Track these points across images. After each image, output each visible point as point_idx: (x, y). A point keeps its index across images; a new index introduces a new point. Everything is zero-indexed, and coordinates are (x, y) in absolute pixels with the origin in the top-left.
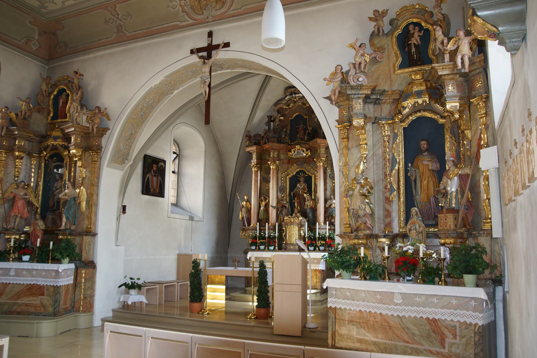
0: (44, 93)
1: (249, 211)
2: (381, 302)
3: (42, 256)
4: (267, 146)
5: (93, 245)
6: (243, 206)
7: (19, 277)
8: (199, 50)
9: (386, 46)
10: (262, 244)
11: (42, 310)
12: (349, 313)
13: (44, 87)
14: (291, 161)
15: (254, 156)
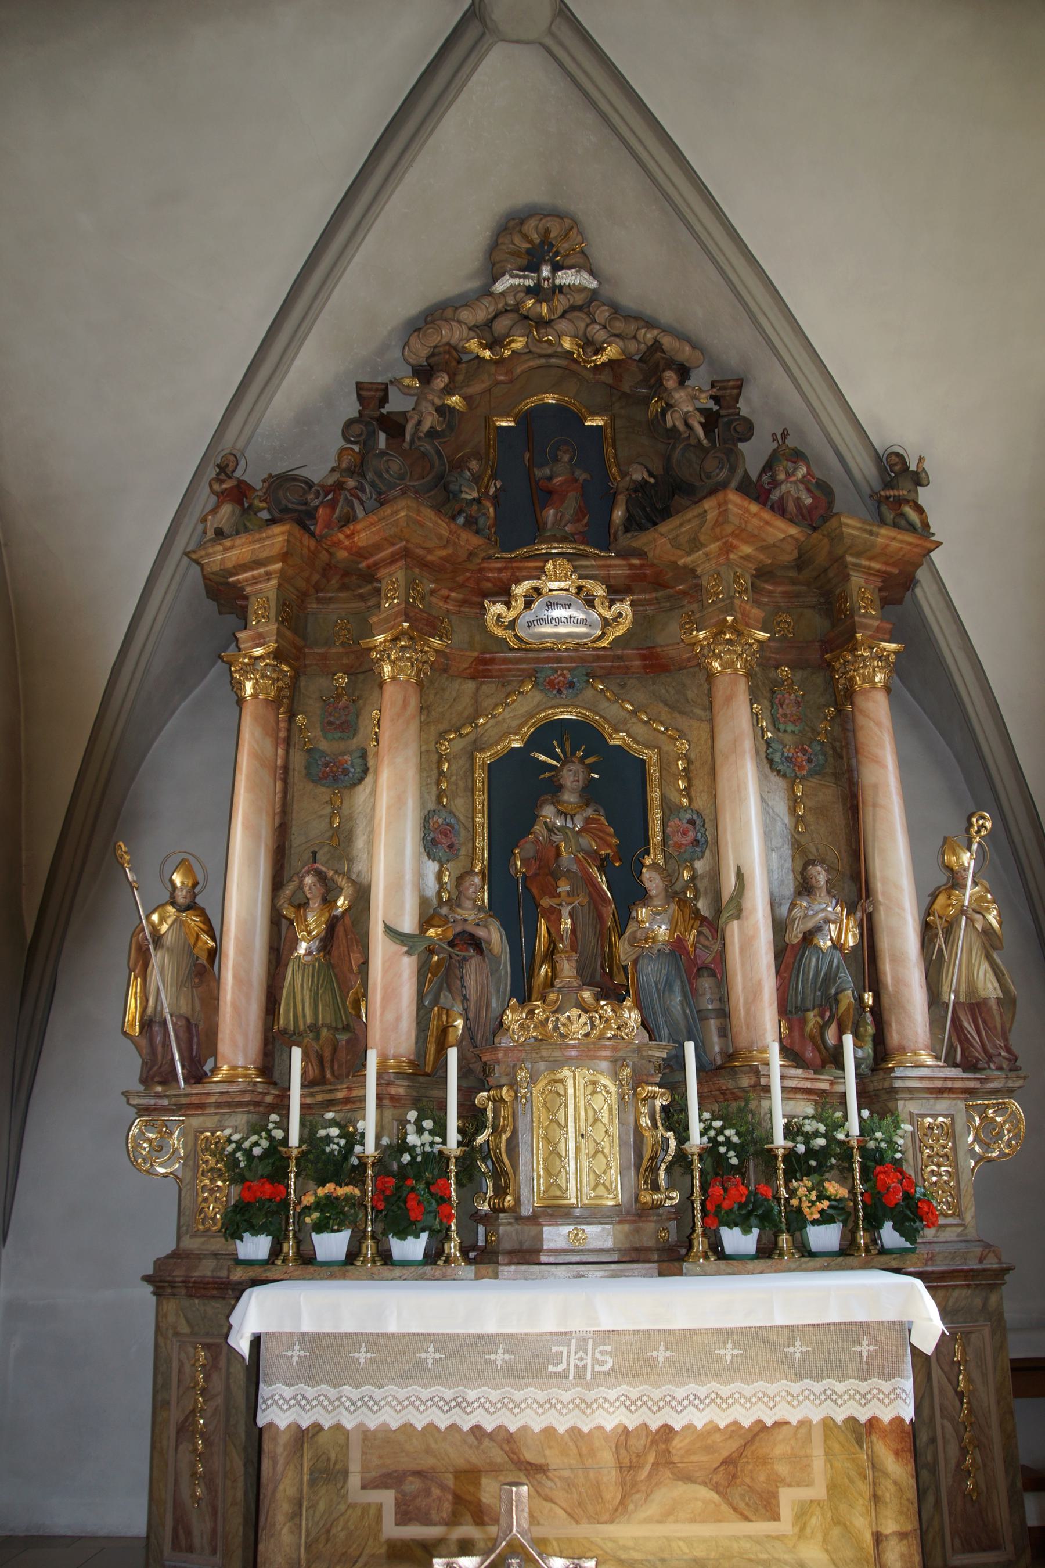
1: (202, 970)
6: (158, 939)
10: (332, 1213)
14: (496, 665)
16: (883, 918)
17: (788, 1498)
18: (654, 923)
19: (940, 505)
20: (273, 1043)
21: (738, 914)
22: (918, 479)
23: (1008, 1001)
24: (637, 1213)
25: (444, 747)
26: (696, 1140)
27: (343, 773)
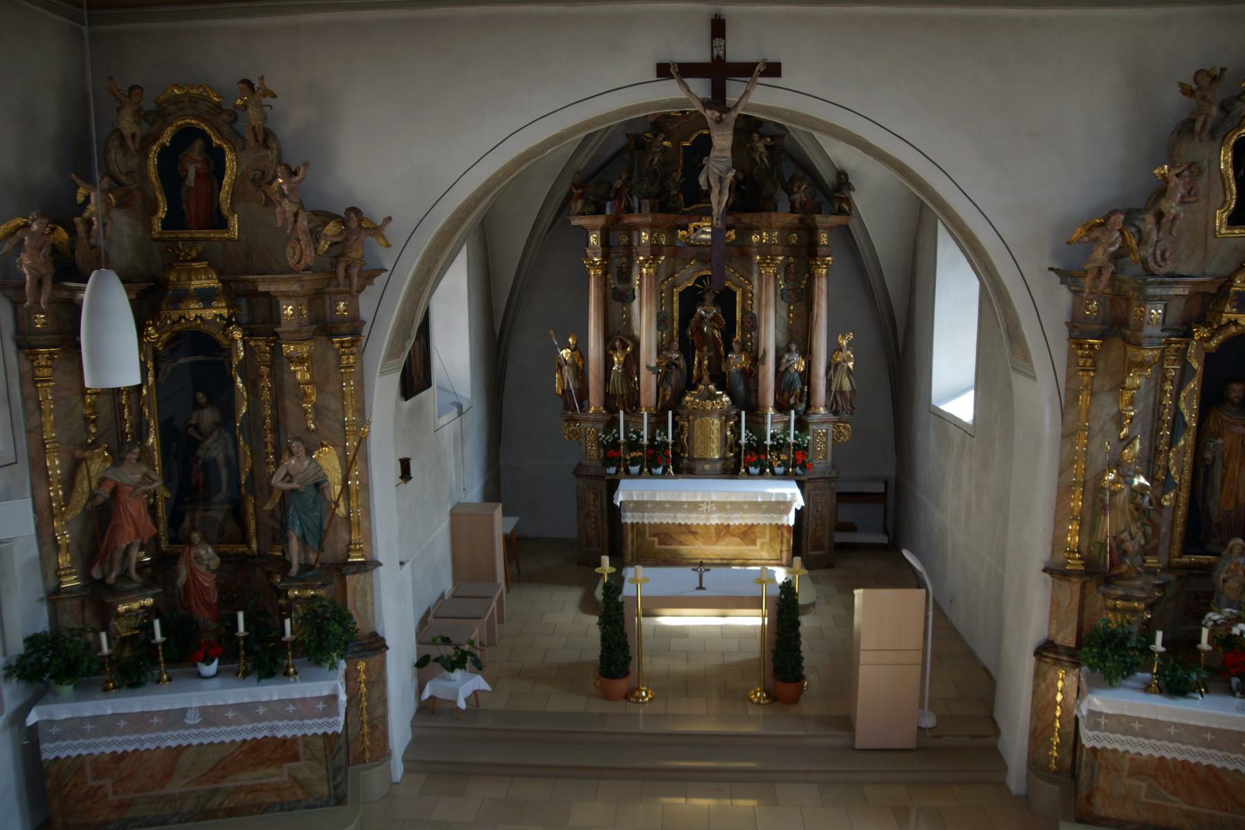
0: (129, 142)
1: (581, 373)
2: (1210, 745)
3: (264, 659)
4: (635, 219)
5: (369, 593)
7: (215, 724)
8: (687, 70)
9: (1205, 164)
11: (300, 795)
12: (1132, 759)
13: (128, 124)
15: (593, 239)
16: (814, 363)
17: (759, 541)
18: (737, 361)
19: (860, 199)
20: (610, 401)
21: (763, 363)
22: (850, 187)
23: (853, 391)
24: (724, 458)
25: (663, 287)
26: (743, 441)
27: (625, 297)
